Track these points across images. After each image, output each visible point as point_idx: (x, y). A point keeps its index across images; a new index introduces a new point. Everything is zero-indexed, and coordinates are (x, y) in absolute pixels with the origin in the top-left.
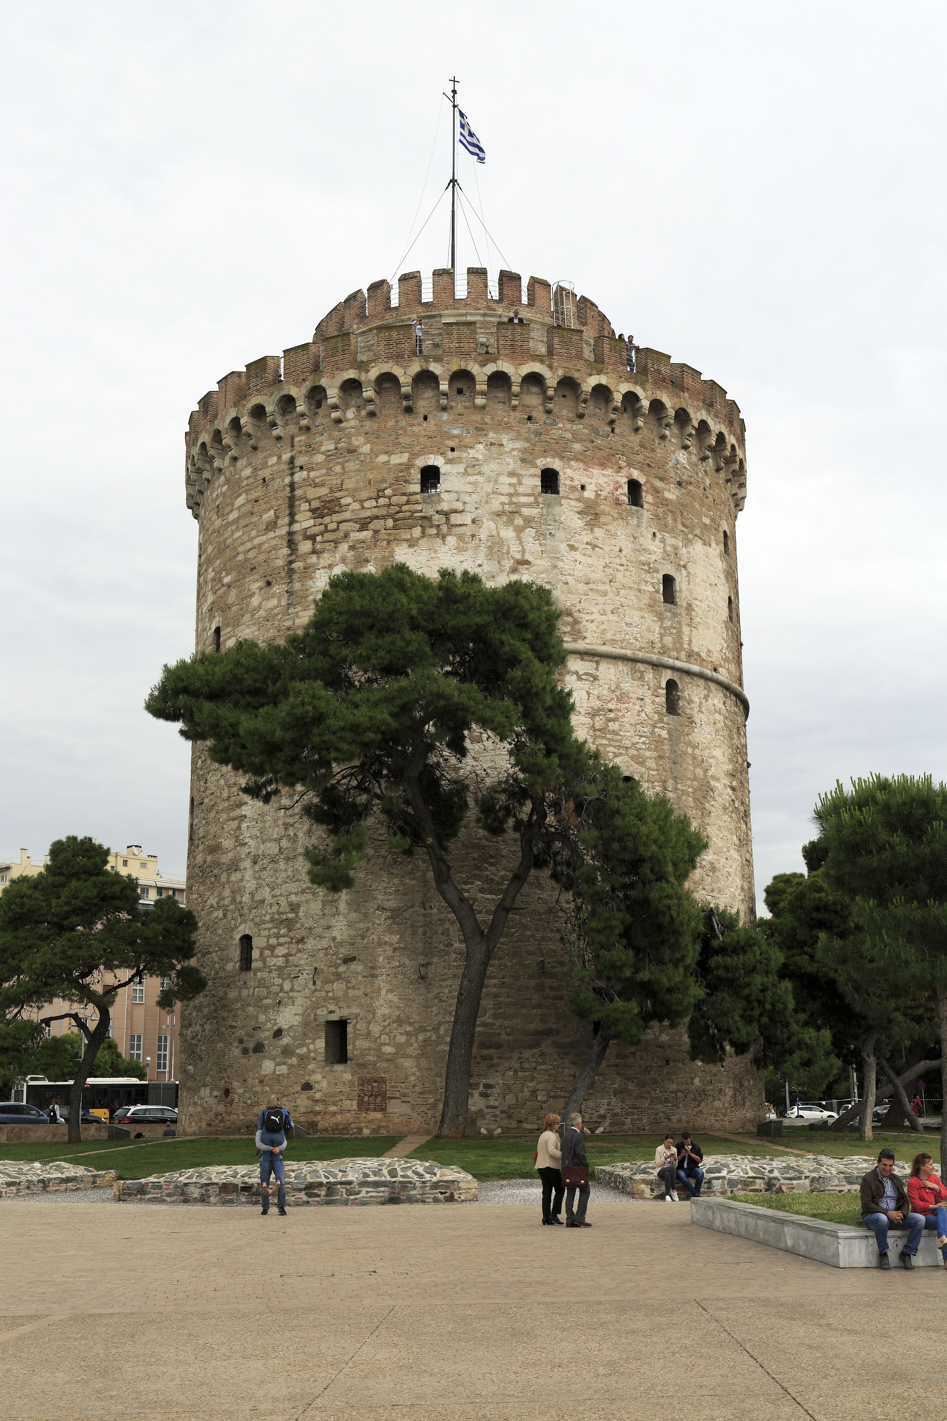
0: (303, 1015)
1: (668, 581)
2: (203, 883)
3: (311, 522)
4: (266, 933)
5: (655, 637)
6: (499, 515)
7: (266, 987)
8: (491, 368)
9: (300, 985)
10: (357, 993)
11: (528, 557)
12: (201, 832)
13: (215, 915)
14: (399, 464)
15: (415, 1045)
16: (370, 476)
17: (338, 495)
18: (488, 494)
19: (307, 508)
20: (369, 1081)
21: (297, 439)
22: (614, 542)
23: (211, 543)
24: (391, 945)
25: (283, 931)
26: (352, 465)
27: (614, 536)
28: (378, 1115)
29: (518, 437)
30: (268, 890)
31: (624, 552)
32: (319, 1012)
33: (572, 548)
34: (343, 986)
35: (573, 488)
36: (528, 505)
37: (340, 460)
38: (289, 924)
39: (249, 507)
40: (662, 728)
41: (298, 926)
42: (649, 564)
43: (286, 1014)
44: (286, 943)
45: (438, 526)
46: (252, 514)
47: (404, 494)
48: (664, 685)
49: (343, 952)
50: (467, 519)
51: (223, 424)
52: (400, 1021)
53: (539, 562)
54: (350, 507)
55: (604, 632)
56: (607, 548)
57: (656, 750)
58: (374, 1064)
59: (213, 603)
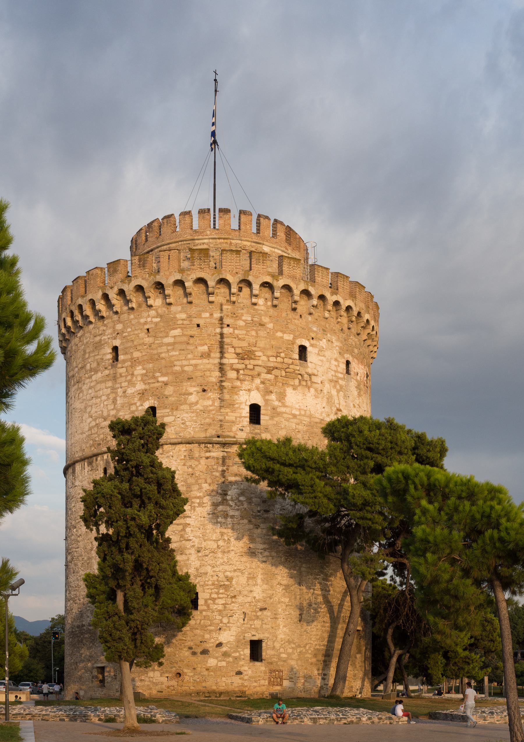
3: (236, 361)
6: (331, 381)
7: (210, 620)
10: (267, 626)
14: (288, 340)
16: (273, 342)
19: (234, 351)
20: (274, 671)
24: (285, 603)
26: (262, 333)
32: (246, 635)
34: (260, 623)
37: (255, 328)
38: (226, 588)
39: (185, 339)
43: (225, 635)
45: (306, 381)
46: (188, 344)
47: (291, 358)
49: (260, 605)
52: (289, 642)
54: (261, 358)
58: (277, 662)
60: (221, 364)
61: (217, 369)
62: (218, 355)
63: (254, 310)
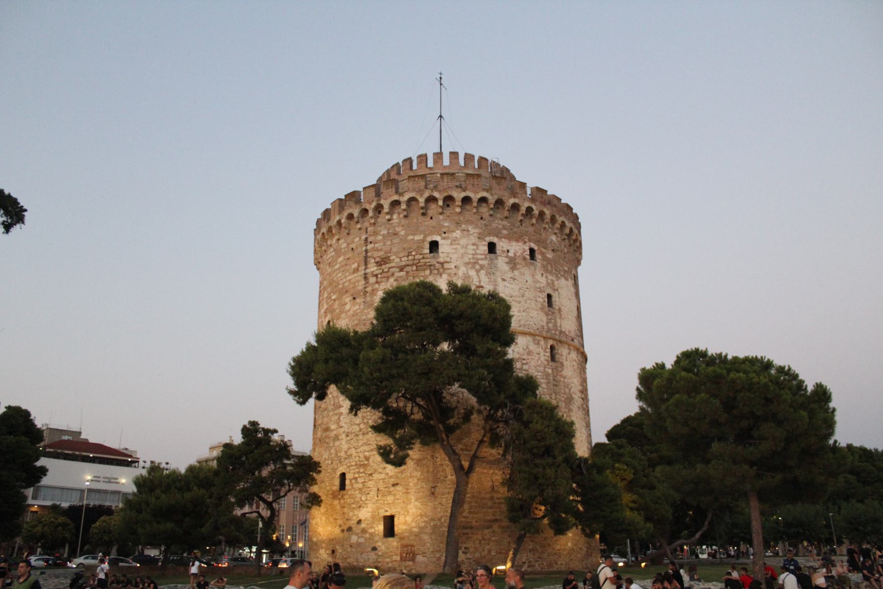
0: (372, 512)
1: (549, 297)
2: (321, 447)
3: (376, 268)
4: (353, 471)
5: (544, 324)
6: (468, 264)
8: (463, 195)
9: (370, 497)
11: (482, 284)
12: (320, 422)
13: (327, 462)
15: (429, 528)
16: (405, 246)
17: (389, 255)
18: (462, 254)
20: (407, 546)
21: (369, 229)
22: (523, 277)
23: (326, 280)
25: (361, 471)
26: (395, 241)
27: (523, 274)
28: (411, 563)
29: (477, 227)
30: (353, 449)
31: (529, 282)
32: (380, 511)
33: (504, 280)
35: (503, 251)
36: (482, 259)
39: (345, 262)
40: (549, 368)
41: (369, 467)
42: (540, 288)
44: (363, 476)
45: (438, 269)
46: (346, 265)
47: (421, 254)
48: (549, 347)
49: (392, 481)
50: (452, 266)
51: (333, 222)
52: (421, 516)
53: (488, 286)
54: (395, 261)
55: (519, 321)
56: (520, 280)
57: (546, 379)
59: (327, 309)
60: (365, 274)
61: (363, 279)
62: (364, 268)
63: (390, 224)
